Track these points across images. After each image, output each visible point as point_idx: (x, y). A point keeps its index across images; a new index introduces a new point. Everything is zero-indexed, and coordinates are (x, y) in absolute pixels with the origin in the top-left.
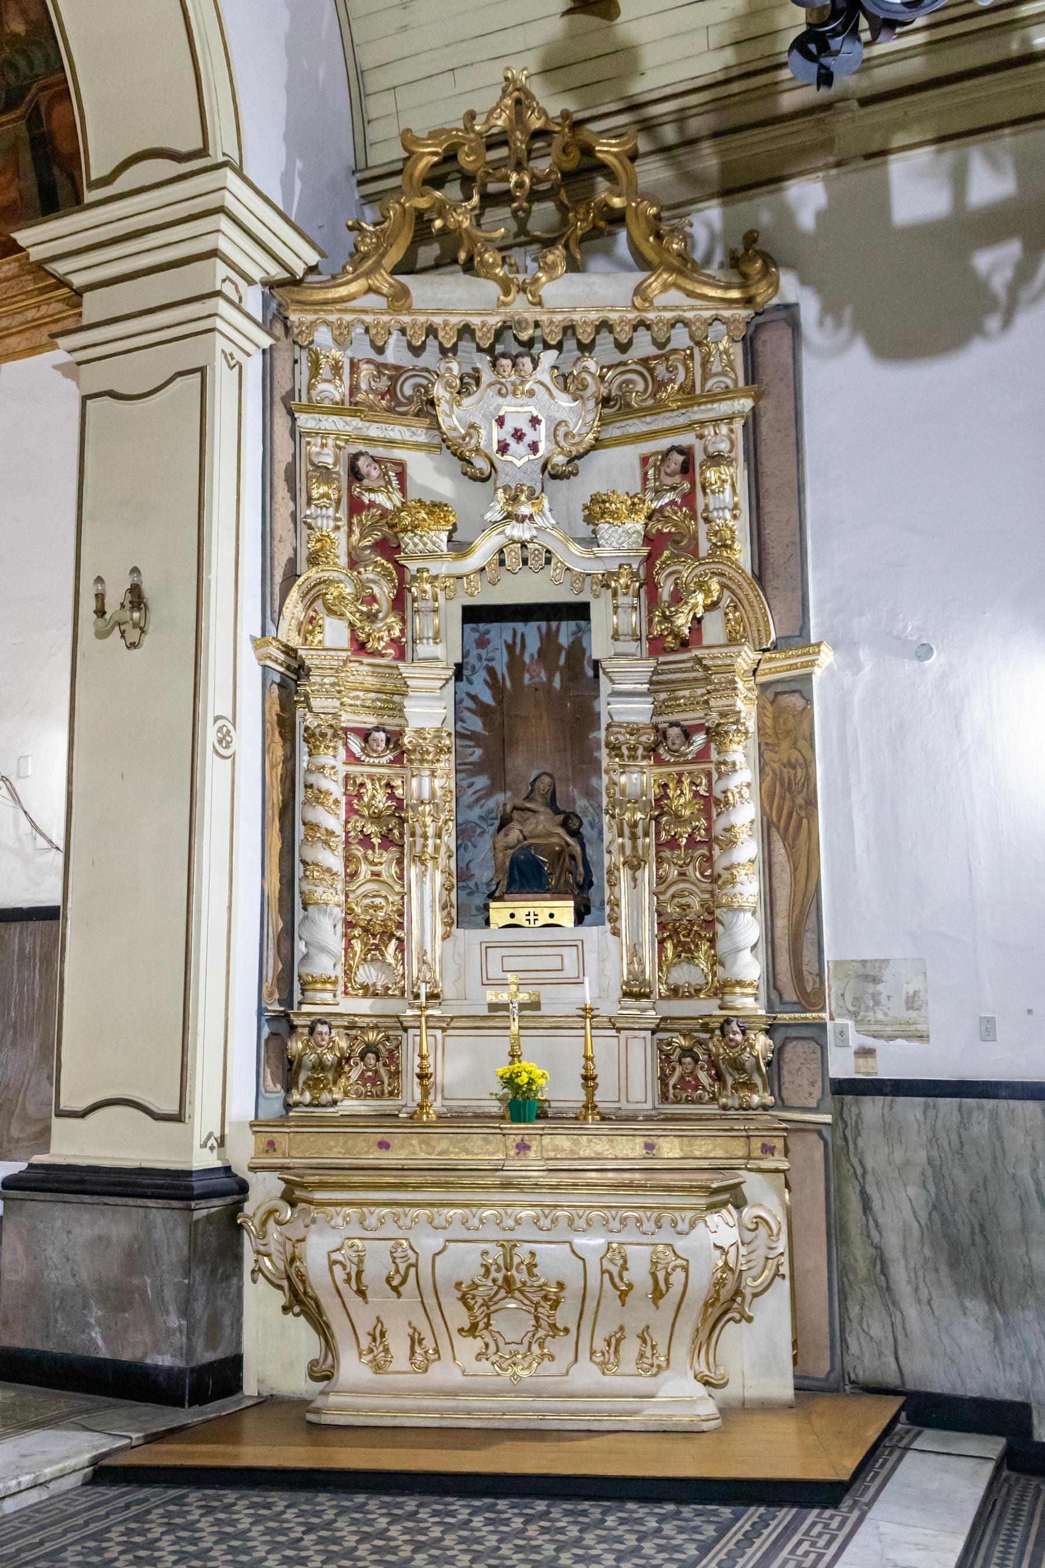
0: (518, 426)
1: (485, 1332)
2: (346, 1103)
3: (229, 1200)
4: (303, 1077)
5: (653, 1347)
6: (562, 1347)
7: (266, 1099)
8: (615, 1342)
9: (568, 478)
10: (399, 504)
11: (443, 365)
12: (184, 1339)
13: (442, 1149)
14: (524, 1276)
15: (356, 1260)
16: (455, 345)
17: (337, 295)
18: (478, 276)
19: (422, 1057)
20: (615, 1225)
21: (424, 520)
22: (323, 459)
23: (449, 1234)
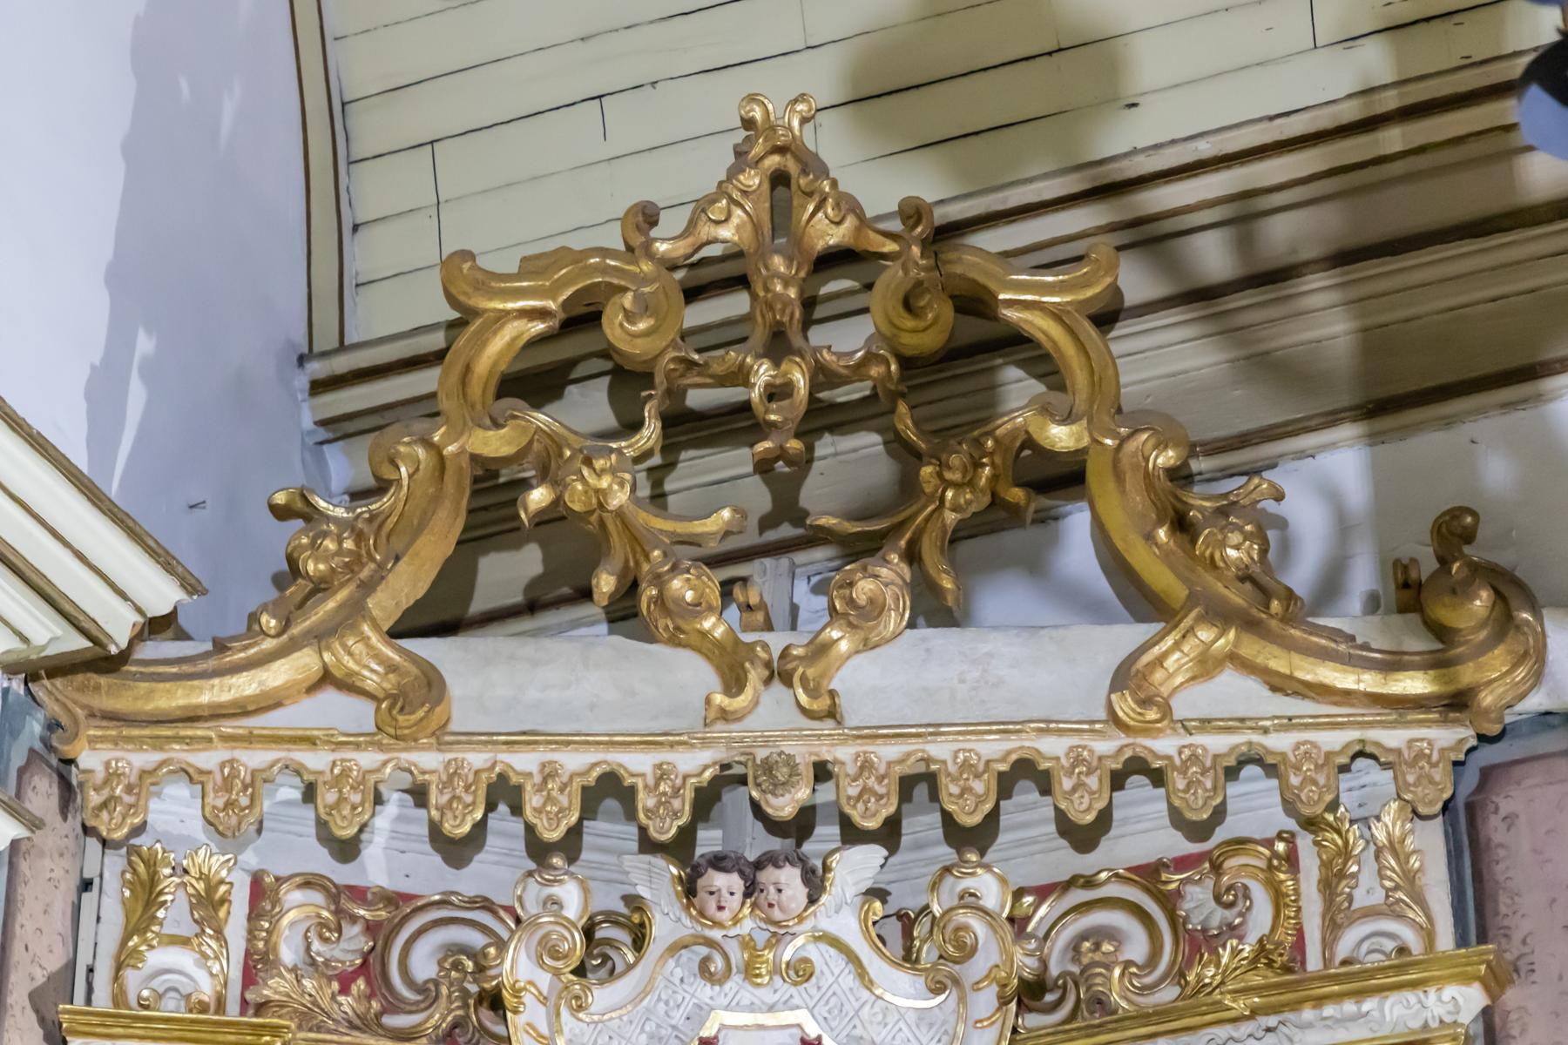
11: (534, 893)
16: (575, 832)
17: (226, 697)
18: (651, 639)
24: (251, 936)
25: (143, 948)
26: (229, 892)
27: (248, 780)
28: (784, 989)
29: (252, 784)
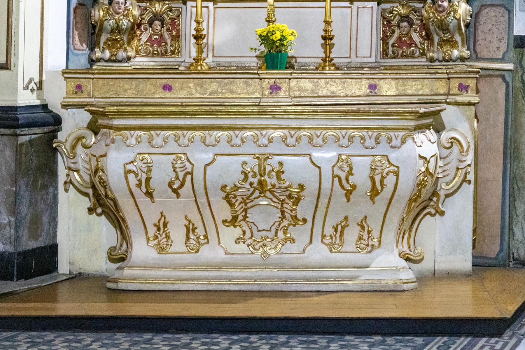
1: (243, 223)
2: (138, 59)
3: (46, 129)
4: (103, 38)
5: (369, 232)
6: (300, 233)
7: (75, 55)
8: (340, 230)
12: (13, 232)
13: (214, 90)
14: (274, 181)
15: (145, 170)
19: (197, 22)
20: (344, 142)
23: (217, 150)
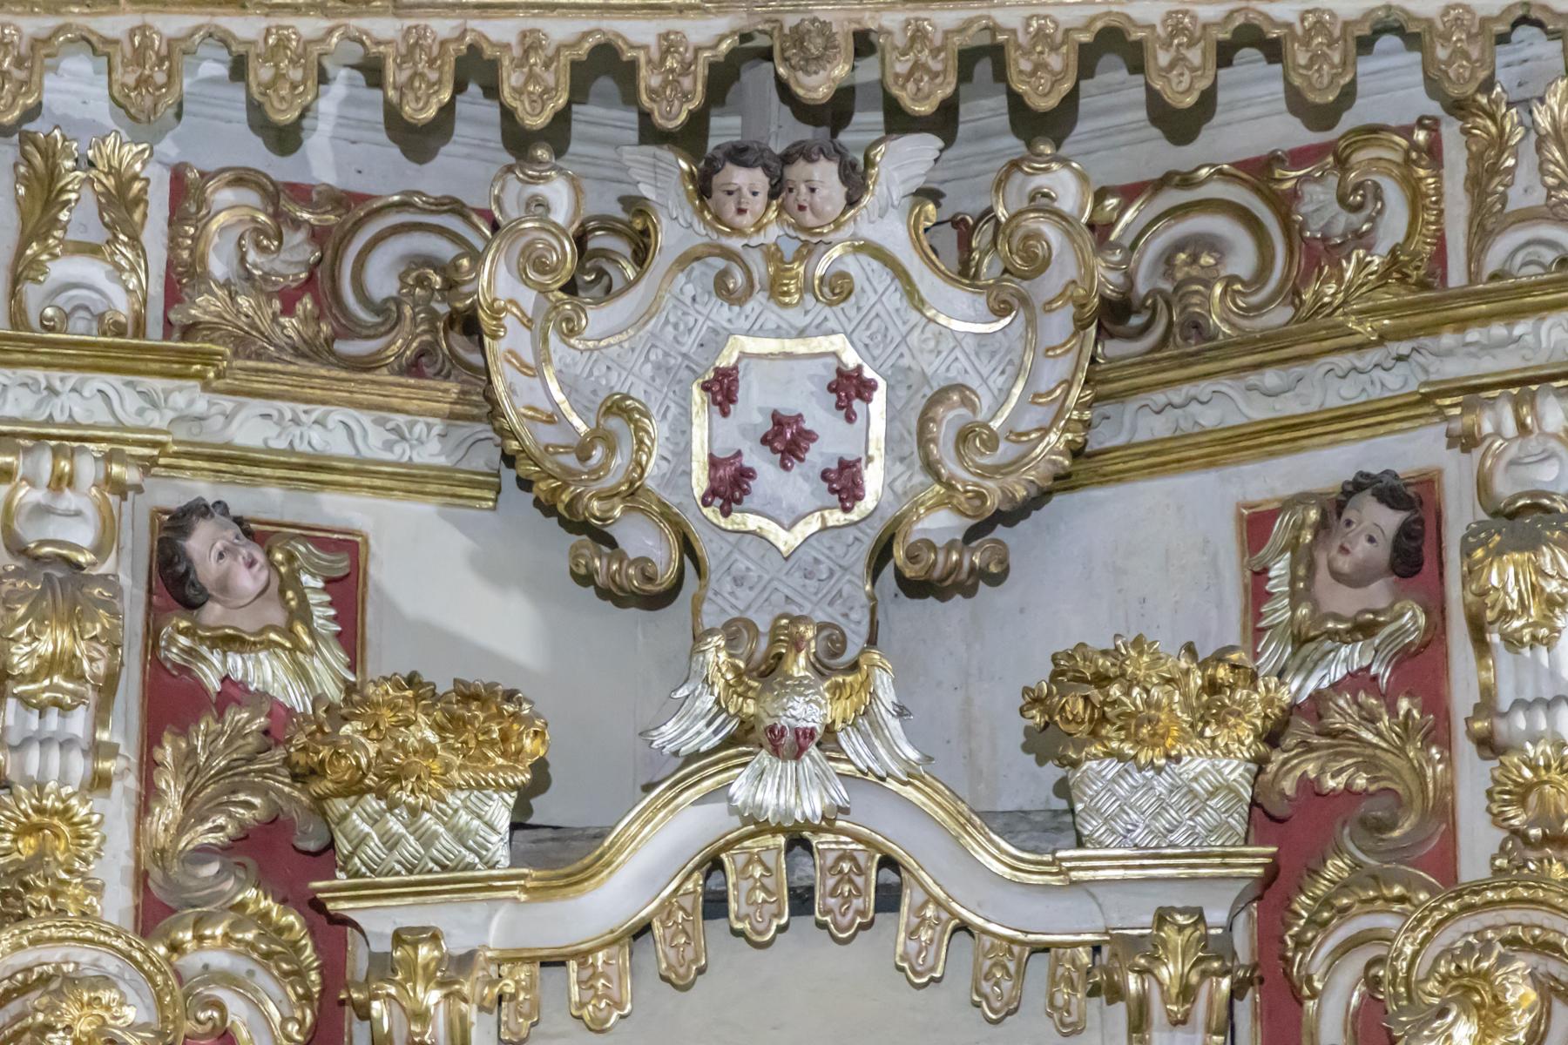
0: (789, 405)
9: (969, 591)
10: (334, 693)
11: (514, 193)
16: (562, 119)
21: (429, 751)
22: (55, 529)
24: (173, 244)
25: (44, 257)
26: (144, 190)
27: (164, 51)
28: (818, 310)
29: (169, 57)
